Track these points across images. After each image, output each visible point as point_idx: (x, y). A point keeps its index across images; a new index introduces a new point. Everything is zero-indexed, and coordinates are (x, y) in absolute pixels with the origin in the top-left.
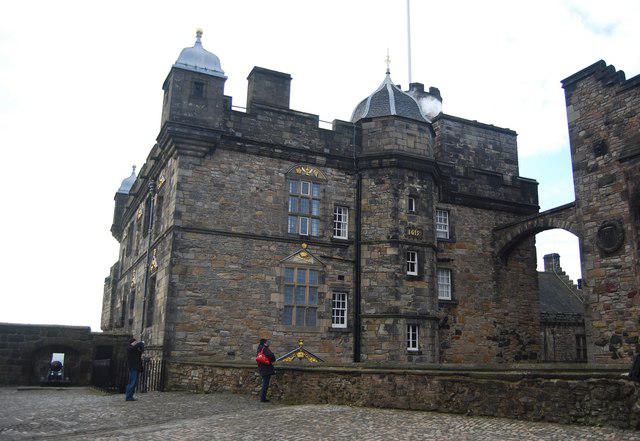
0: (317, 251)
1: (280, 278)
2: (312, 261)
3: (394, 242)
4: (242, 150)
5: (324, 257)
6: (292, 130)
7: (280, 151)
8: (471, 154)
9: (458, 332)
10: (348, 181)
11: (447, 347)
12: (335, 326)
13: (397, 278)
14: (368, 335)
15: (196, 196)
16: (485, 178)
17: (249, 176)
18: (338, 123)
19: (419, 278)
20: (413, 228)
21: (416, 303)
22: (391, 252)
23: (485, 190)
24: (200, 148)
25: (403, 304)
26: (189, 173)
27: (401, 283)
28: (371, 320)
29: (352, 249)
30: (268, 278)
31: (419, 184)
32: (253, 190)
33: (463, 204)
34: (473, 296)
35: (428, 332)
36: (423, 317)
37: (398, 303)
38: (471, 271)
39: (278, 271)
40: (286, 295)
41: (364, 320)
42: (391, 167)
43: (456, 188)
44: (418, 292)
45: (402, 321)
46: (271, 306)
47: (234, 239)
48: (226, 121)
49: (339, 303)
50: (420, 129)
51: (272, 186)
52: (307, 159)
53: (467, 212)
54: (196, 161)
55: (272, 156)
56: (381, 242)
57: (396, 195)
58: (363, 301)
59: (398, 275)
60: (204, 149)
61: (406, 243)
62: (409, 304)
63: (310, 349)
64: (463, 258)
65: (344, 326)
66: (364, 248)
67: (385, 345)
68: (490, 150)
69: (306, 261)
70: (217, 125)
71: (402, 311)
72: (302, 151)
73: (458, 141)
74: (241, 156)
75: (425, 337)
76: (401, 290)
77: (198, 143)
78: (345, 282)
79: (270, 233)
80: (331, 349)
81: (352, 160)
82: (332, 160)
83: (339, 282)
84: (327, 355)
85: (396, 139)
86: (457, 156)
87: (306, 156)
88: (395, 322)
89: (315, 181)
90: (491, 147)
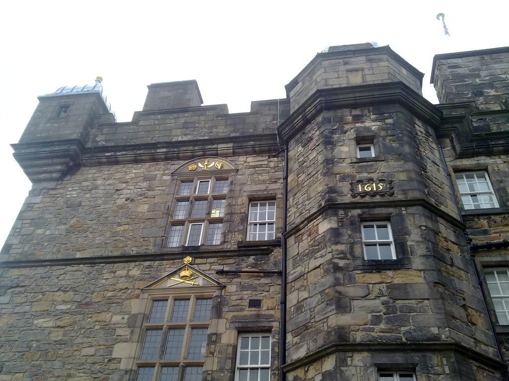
0: (212, 266)
1: (134, 317)
2: (200, 282)
3: (330, 207)
4: (116, 162)
7: (165, 150)
10: (272, 164)
13: (337, 268)
15: (38, 222)
17: (125, 192)
18: (259, 107)
19: (398, 265)
20: (371, 180)
22: (324, 226)
24: (52, 168)
26: (38, 199)
27: (352, 280)
29: (277, 253)
30: (117, 319)
31: (374, 121)
32: (121, 201)
36: (425, 346)
37: (344, 320)
39: (137, 306)
40: (141, 340)
42: (318, 113)
44: (398, 292)
45: (359, 359)
46: (112, 366)
47: (76, 268)
48: (96, 136)
49: (255, 356)
50: (370, 61)
51: (150, 193)
54: (52, 184)
55: (154, 159)
56: (310, 219)
57: (328, 142)
58: (289, 337)
59: (341, 263)
60: (59, 167)
62: (377, 320)
70: (74, 137)
71: (359, 337)
73: (478, 76)
74: (114, 168)
76: (350, 290)
77: (49, 161)
78: (264, 310)
79: (134, 251)
83: (249, 312)
85: (326, 80)
86: (481, 94)
88: (341, 363)
89: (220, 176)
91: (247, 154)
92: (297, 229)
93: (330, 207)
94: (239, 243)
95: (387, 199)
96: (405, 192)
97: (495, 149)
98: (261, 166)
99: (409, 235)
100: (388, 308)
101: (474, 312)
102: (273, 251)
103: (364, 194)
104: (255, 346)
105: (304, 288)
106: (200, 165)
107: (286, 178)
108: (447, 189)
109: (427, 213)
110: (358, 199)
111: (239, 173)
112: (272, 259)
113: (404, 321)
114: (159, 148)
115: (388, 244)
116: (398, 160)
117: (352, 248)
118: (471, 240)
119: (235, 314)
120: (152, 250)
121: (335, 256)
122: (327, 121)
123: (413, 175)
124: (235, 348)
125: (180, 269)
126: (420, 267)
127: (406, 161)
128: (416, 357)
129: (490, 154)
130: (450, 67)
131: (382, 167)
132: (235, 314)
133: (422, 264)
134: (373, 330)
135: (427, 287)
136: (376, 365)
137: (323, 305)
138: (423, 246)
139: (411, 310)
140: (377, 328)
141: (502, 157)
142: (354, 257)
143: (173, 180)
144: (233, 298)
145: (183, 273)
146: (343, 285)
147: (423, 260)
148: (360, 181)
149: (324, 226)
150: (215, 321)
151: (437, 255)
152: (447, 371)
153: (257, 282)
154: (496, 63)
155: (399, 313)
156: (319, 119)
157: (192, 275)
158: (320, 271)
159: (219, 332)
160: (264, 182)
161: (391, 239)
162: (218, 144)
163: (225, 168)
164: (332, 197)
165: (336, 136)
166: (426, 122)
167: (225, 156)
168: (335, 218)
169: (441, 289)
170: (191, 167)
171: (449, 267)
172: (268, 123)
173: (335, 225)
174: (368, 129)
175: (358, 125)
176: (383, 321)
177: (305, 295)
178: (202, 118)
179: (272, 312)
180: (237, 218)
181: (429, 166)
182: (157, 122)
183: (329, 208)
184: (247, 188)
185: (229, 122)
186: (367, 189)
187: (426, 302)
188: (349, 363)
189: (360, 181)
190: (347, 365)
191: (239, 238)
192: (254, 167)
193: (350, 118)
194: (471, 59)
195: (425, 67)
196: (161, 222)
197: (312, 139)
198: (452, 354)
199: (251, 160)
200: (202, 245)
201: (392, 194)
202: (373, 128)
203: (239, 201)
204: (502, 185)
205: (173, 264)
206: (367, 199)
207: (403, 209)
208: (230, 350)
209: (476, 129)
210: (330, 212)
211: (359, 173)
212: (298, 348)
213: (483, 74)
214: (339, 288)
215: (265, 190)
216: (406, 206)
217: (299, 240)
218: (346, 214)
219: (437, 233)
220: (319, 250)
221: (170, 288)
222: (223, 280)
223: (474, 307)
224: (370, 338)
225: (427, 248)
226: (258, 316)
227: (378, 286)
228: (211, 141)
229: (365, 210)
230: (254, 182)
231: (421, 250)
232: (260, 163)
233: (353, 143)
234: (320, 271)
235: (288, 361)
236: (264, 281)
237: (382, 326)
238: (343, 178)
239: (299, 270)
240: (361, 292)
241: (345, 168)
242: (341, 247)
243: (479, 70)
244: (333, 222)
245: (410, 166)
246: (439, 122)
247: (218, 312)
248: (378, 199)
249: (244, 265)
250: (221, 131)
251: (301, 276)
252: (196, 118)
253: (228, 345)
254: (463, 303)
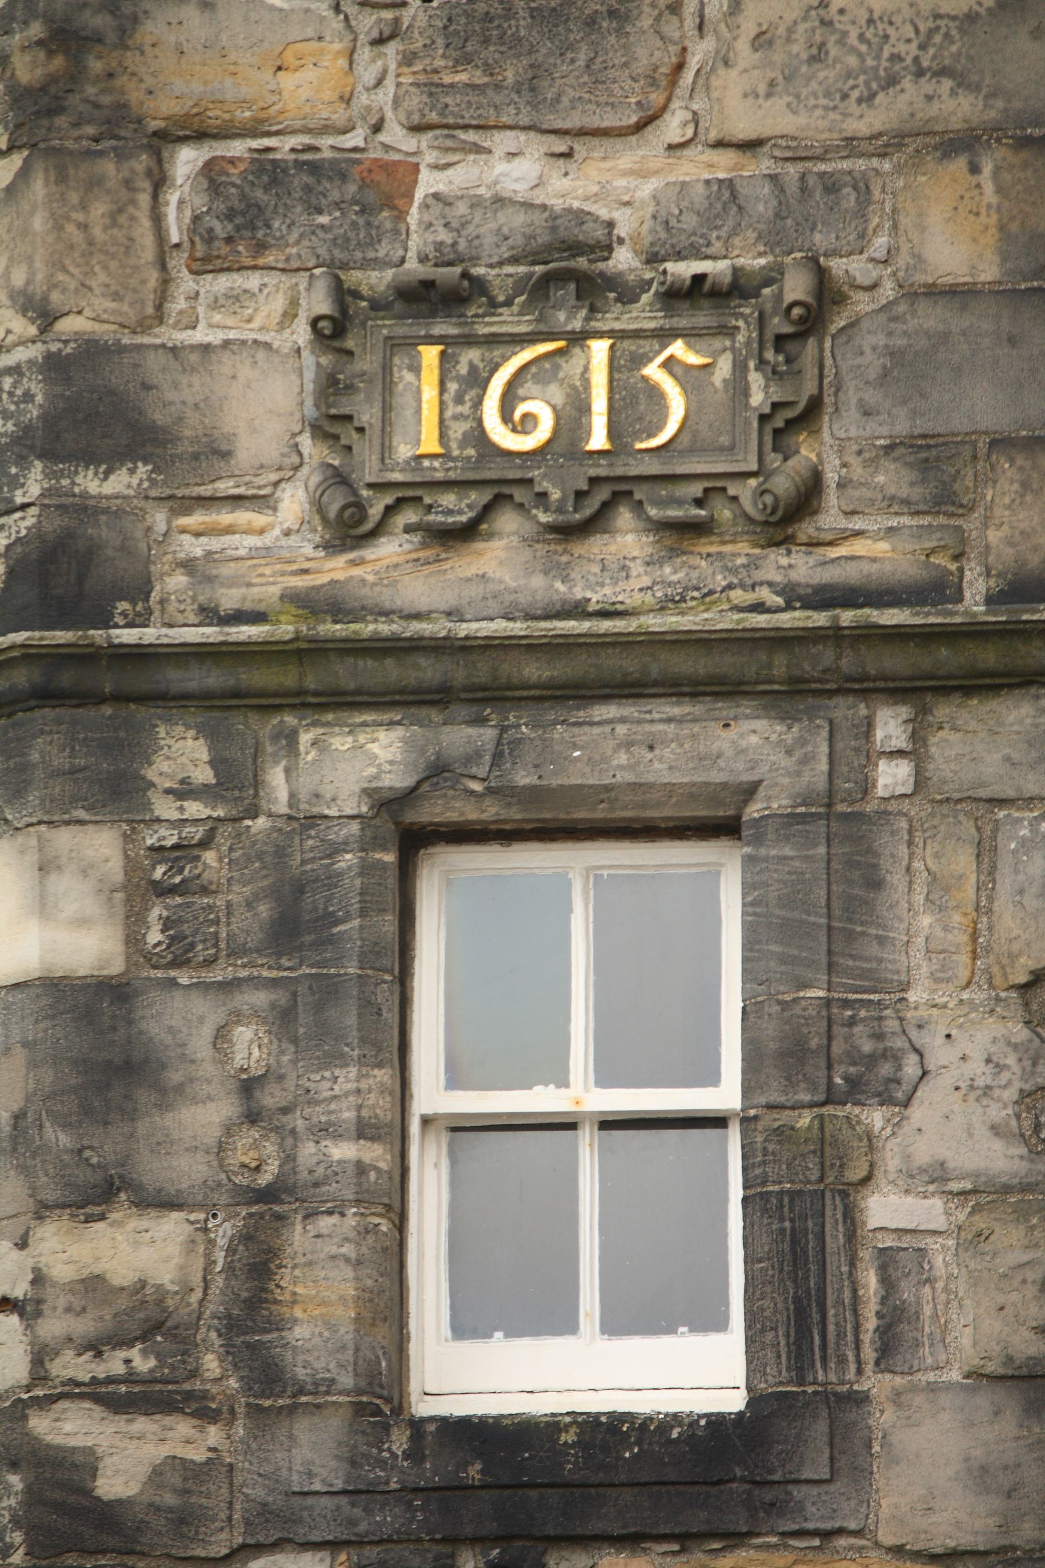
61: (327, 668)
95: (735, 587)
96: (939, 471)
99: (897, 1097)
115: (717, 1121)
121: (73, 1366)
148: (440, 299)
161: (726, 1095)
164: (85, 509)
168: (101, 846)
173: (89, 947)
183: (45, 696)
189: (440, 299)
201: (787, 518)
207: (890, 726)
211: (452, 125)
218: (235, 782)
229: (461, 736)
242: (147, 1251)
244: (74, 893)
248: (625, 573)
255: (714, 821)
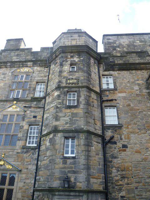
0: (22, 104)
2: (18, 109)
5: (25, 107)
6: (17, 55)
7: (10, 64)
8: (124, 47)
9: (125, 146)
10: (45, 70)
11: (116, 158)
12: (27, 145)
13: (57, 107)
14: (43, 148)
16: (135, 54)
18: (43, 49)
20: (72, 79)
21: (72, 122)
22: (56, 93)
23: (135, 59)
25: (62, 124)
27: (61, 111)
28: (44, 138)
29: (43, 101)
31: (77, 58)
33: (120, 69)
34: (135, 121)
35: (82, 142)
36: (78, 131)
37: (57, 123)
38: (132, 105)
41: (42, 139)
42: (60, 53)
43: (114, 62)
45: (60, 135)
50: (79, 36)
51: (4, 79)
52: (23, 64)
53: (125, 73)
57: (61, 65)
58: (43, 127)
59: (59, 106)
61: (65, 87)
62: (67, 123)
63: (9, 160)
64: (124, 98)
65: (36, 145)
66: (47, 98)
67: (48, 153)
68: (138, 43)
69: (15, 110)
71: (61, 128)
72: (20, 62)
73: (115, 43)
75: (79, 145)
76: (60, 114)
80: (23, 160)
81: (46, 60)
82: (35, 62)
83: (33, 119)
84: (20, 163)
85: (64, 42)
86: (115, 49)
87: (23, 64)
88: (55, 136)
90: (138, 42)
91: (37, 66)
92: (49, 94)
93: (58, 88)
94: (32, 97)
95: (76, 85)
96: (82, 83)
97: (115, 69)
98: (42, 71)
100: (70, 120)
101: (97, 121)
102: (42, 100)
103: (70, 83)
104: (34, 130)
105: (48, 113)
106: (21, 70)
107: (49, 76)
108: (98, 82)
109: (88, 90)
110: (67, 85)
111: (34, 73)
112: (42, 103)
113: (75, 124)
114: (8, 63)
116: (82, 72)
117: (63, 101)
118: (103, 98)
119: (29, 120)
120: (4, 99)
122: (62, 57)
123: (86, 78)
124: (28, 130)
125: (12, 105)
126: (82, 108)
127: (84, 73)
128: (76, 134)
129: (113, 70)
130: (107, 39)
131: (77, 75)
132: (29, 120)
133: (83, 106)
134: (65, 126)
135: (82, 114)
136: (64, 136)
137: (52, 119)
138: (84, 101)
139: (77, 120)
140: (66, 126)
141: (117, 72)
142: (63, 104)
143: (12, 75)
144: (28, 115)
145: (13, 107)
146: (59, 113)
147: (84, 105)
148: (69, 79)
149: (56, 93)
150: (22, 122)
151: (88, 104)
152: (84, 138)
153: (36, 110)
154: (122, 39)
155: (73, 121)
156: (60, 56)
157: (16, 107)
158: (53, 108)
159: (23, 125)
160: (42, 76)
161: (76, 98)
162: (28, 62)
163: (30, 71)
165: (64, 63)
166: (95, 59)
167: (30, 67)
169: (87, 114)
170: (18, 70)
171: (92, 107)
172: (45, 55)
173: (59, 94)
174: (75, 61)
175: (72, 59)
176: (68, 124)
177: (48, 115)
178: (23, 53)
179: (40, 120)
180: (32, 89)
181: (93, 74)
182: (8, 54)
183: (58, 88)
184: (36, 79)
185: (32, 54)
186: (71, 82)
187: (82, 118)
188: (57, 136)
189: (69, 79)
190: (56, 136)
191: (32, 96)
192: (39, 71)
193: (70, 56)
194: (114, 37)
195: (99, 39)
196: (7, 89)
197: (57, 63)
198: (86, 134)
199: (39, 69)
200: (20, 98)
202: (76, 61)
203: (33, 83)
204: (115, 81)
205: (10, 104)
206: (70, 85)
208: (26, 131)
209: (111, 62)
210: (58, 89)
211: (69, 76)
212: (45, 131)
213: (117, 42)
214: (57, 114)
215: (42, 80)
216: (81, 88)
217: (49, 98)
218: (63, 90)
219: (90, 97)
220: (54, 101)
221: (9, 111)
222: (26, 109)
223: (97, 119)
224: (64, 129)
225: (85, 102)
226: (35, 121)
227: (69, 113)
228: (26, 62)
229: (69, 89)
230: (38, 76)
231: (83, 102)
232: (42, 70)
233: (69, 65)
234: (53, 108)
235: (42, 134)
236: (38, 110)
237: (68, 125)
238: (64, 78)
239: (48, 107)
240: (63, 115)
241: (65, 74)
242: (60, 101)
243: (116, 41)
245: (85, 74)
246: (100, 59)
247: (23, 120)
248: (74, 85)
249: (33, 104)
250: (29, 58)
251: (48, 109)
252: (21, 53)
253: (26, 129)
254: (94, 118)
255: (76, 92)
